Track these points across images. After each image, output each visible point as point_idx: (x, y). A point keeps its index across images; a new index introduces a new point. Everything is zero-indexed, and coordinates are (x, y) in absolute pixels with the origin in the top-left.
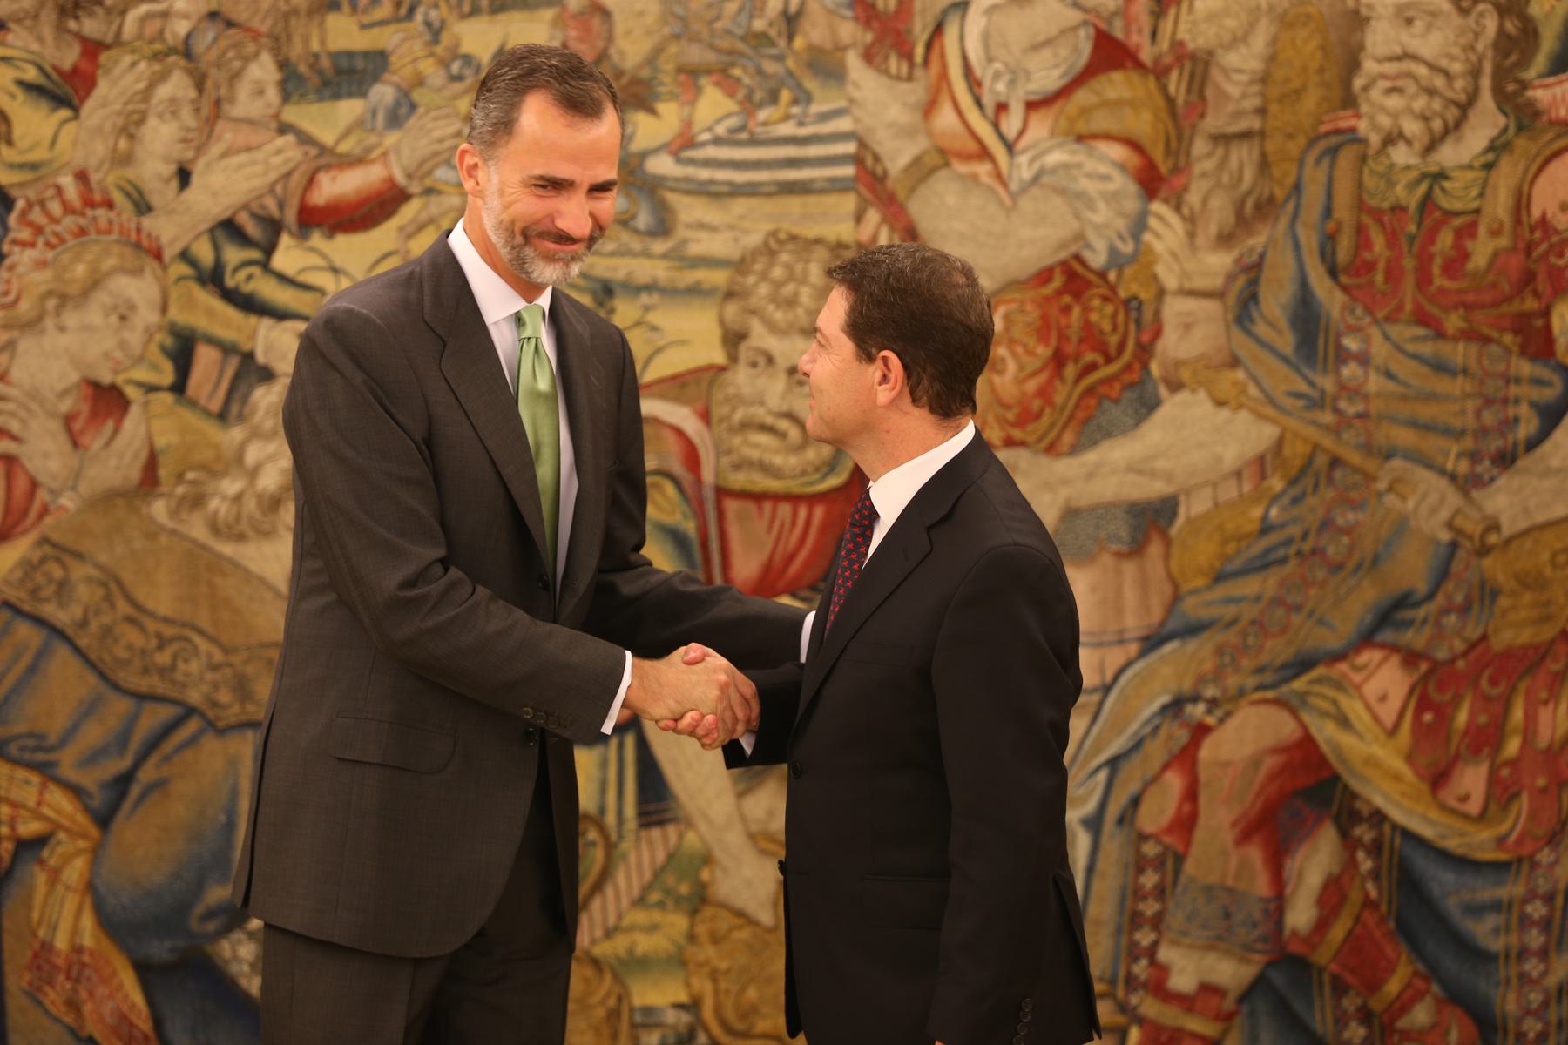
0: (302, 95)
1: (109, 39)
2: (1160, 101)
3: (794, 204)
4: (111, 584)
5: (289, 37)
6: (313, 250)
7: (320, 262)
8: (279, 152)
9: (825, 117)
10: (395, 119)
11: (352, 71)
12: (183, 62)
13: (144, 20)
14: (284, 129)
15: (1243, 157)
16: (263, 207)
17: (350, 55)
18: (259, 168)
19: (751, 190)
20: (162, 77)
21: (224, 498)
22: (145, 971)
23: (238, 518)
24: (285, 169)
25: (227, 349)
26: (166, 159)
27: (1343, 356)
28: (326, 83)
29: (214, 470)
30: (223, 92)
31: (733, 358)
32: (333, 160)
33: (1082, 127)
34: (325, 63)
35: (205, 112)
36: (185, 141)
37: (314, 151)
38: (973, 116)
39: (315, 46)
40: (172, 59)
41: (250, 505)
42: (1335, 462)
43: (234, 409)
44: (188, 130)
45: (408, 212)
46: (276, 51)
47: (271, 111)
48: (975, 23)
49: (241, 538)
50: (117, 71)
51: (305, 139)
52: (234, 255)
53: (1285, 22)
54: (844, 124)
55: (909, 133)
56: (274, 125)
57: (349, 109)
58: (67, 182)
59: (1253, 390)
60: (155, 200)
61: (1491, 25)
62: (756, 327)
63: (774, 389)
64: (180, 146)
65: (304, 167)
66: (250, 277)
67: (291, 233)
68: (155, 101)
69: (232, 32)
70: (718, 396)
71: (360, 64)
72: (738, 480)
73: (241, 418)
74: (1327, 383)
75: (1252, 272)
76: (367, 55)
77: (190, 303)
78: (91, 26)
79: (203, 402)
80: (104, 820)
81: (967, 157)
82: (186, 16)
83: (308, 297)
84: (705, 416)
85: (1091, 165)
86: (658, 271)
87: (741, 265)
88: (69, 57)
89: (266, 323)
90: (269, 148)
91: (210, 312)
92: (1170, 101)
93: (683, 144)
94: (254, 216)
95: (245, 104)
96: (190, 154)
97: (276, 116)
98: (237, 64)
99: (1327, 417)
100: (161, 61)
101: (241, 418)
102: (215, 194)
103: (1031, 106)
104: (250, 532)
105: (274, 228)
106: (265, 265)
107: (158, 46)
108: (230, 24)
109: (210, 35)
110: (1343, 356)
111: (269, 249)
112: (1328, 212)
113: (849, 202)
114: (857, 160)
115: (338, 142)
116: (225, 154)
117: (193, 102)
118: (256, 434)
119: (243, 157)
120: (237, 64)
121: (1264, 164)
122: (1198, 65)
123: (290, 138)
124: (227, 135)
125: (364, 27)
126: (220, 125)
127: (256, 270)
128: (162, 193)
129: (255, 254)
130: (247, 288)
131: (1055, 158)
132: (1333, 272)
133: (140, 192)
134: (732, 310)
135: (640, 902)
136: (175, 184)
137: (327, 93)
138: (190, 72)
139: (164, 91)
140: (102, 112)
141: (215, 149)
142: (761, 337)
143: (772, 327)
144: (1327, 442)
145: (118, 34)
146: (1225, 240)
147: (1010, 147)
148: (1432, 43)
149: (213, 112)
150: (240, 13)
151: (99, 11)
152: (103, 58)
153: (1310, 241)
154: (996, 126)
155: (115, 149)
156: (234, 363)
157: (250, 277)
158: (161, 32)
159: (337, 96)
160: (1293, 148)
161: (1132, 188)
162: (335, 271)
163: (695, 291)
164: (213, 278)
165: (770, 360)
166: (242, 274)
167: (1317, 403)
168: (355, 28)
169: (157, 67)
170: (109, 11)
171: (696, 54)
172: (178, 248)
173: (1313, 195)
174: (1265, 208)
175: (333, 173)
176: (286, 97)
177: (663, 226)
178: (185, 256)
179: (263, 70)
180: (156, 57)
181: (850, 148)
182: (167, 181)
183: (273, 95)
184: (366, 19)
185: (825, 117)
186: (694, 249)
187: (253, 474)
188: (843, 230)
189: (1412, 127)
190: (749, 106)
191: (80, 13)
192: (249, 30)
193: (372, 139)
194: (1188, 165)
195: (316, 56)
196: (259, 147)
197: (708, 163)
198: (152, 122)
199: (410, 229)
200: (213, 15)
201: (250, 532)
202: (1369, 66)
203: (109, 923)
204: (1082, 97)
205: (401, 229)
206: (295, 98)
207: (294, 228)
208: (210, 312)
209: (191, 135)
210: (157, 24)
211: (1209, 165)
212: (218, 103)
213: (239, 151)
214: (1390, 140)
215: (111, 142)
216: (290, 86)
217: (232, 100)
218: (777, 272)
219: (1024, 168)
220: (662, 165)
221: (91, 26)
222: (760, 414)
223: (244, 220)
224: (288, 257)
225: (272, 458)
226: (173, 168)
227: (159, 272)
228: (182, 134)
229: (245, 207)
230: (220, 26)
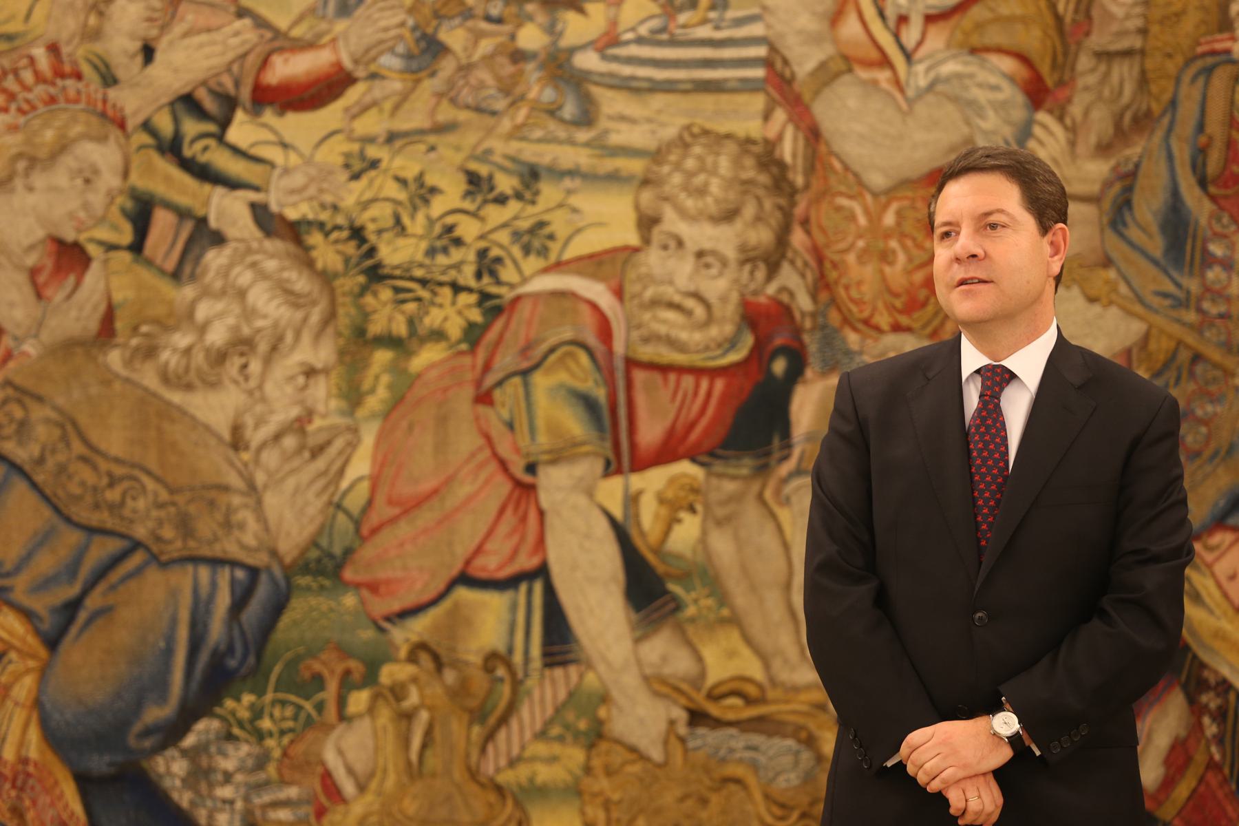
2: (1049, 20)
3: (708, 102)
4: (68, 425)
7: (271, 137)
9: (739, 22)
15: (1124, 73)
16: (220, 84)
19: (668, 87)
21: (175, 350)
22: (84, 782)
23: (187, 369)
24: (241, 50)
25: (183, 214)
26: (132, 36)
27: (1209, 260)
29: (167, 325)
31: (647, 241)
32: (286, 44)
33: (975, 40)
36: (150, 20)
37: (269, 35)
41: (199, 358)
42: (1197, 358)
43: (187, 269)
44: (154, 10)
45: (353, 95)
49: (189, 387)
51: (261, 23)
52: (191, 127)
54: (757, 30)
55: (814, 39)
58: (40, 53)
59: (1123, 289)
60: (120, 73)
62: (669, 214)
63: (683, 271)
65: (258, 50)
66: (206, 149)
67: (245, 109)
70: (631, 274)
72: (646, 352)
73: (193, 277)
74: (1193, 285)
75: (1127, 179)
77: (149, 170)
79: (158, 261)
80: (52, 642)
81: (868, 64)
83: (258, 168)
84: (619, 293)
85: (983, 76)
86: (581, 158)
87: (657, 156)
89: (220, 191)
90: (228, 30)
91: (168, 179)
92: (1059, 19)
93: (608, 42)
94: (212, 92)
96: (154, 32)
99: (1191, 316)
101: (193, 277)
102: (176, 71)
103: (930, 19)
104: (197, 382)
105: (230, 104)
106: (220, 138)
110: (1209, 260)
111: (225, 123)
112: (1201, 128)
113: (758, 102)
114: (767, 63)
118: (206, 293)
119: (204, 38)
121: (1143, 81)
123: (247, 22)
127: (212, 142)
128: (127, 67)
129: (211, 127)
130: (203, 158)
131: (949, 68)
132: (1203, 183)
133: (107, 66)
134: (647, 196)
135: (542, 735)
136: (139, 59)
141: (178, 29)
142: (672, 222)
143: (683, 213)
144: (1190, 339)
146: (1103, 149)
147: (908, 56)
153: (1182, 153)
154: (897, 36)
156: (188, 227)
157: (206, 149)
160: (1171, 67)
161: (1020, 98)
162: (285, 146)
163: (614, 178)
164: (172, 148)
165: (680, 243)
166: (199, 146)
167: (1182, 303)
172: (140, 119)
173: (1188, 111)
174: (1142, 122)
175: (287, 55)
177: (586, 118)
178: (147, 126)
181: (761, 51)
182: (133, 56)
185: (739, 22)
186: (615, 139)
187: (203, 329)
188: (752, 127)
193: (323, 26)
194: (1073, 79)
196: (218, 28)
197: (631, 60)
199: (355, 110)
201: (197, 382)
203: (54, 738)
205: (347, 110)
207: (248, 104)
208: (168, 179)
211: (1091, 79)
218: (690, 163)
219: (920, 77)
220: (588, 61)
222: (669, 292)
223: (203, 95)
224: (241, 131)
225: (220, 315)
226: (138, 45)
227: (122, 140)
229: (204, 83)
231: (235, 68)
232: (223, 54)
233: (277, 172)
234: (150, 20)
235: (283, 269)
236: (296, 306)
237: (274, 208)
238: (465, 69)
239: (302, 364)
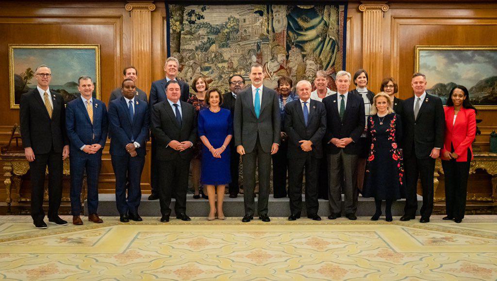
10: (212, 73)
20: (189, 69)
38: (268, 73)
48: (269, 64)
53: (299, 65)
57: (207, 72)
61: (319, 65)
78: (183, 64)
88: (181, 66)
95: (197, 71)
103: (274, 72)
122: (290, 69)
128: (189, 80)
139: (189, 70)
148: (313, 67)
149: (194, 72)
171: (241, 67)
179: (199, 68)
189: (311, 75)
190: (246, 72)
202: (307, 69)
204: (279, 72)
214: (309, 77)
221: (183, 64)
238: (225, 79)
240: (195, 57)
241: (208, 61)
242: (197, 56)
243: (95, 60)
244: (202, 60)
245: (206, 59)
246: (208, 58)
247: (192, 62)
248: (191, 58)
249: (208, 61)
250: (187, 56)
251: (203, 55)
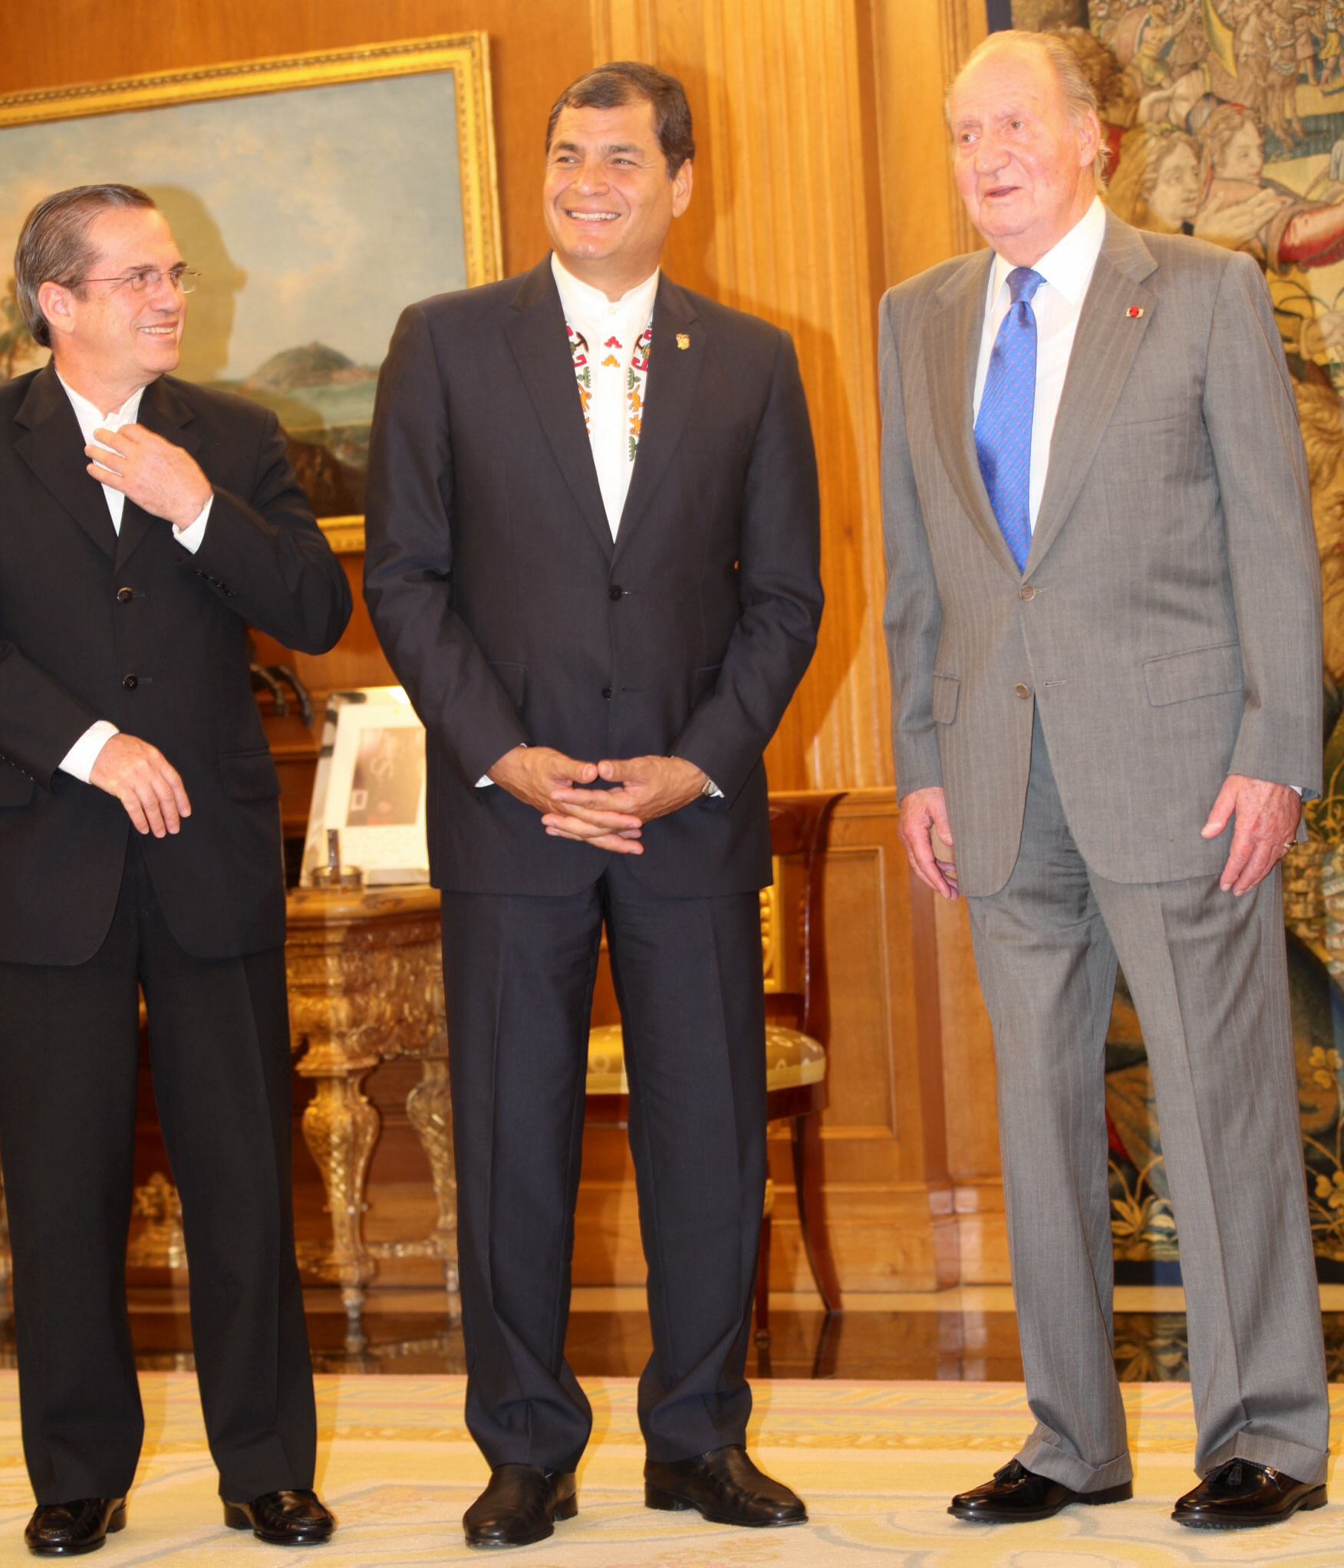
0: (1278, 156)
1: (1128, 123)
5: (1267, 108)
6: (1292, 282)
7: (1300, 293)
8: (1261, 204)
11: (1318, 132)
12: (1185, 137)
13: (1152, 106)
14: (1265, 183)
17: (1317, 118)
18: (1246, 218)
20: (1168, 150)
28: (1298, 144)
30: (1216, 158)
32: (1305, 207)
34: (1296, 126)
35: (1203, 175)
36: (1187, 200)
37: (1289, 201)
39: (1288, 114)
40: (1176, 134)
44: (1191, 191)
46: (1257, 121)
47: (1255, 170)
50: (1134, 148)
51: (1282, 191)
56: (1257, 182)
57: (1317, 163)
64: (1185, 205)
67: (1273, 270)
68: (1163, 170)
69: (1222, 108)
71: (1324, 125)
76: (1329, 116)
82: (1186, 99)
83: (1290, 321)
90: (1254, 200)
96: (1192, 211)
97: (1259, 174)
98: (1226, 134)
100: (1166, 138)
107: (1165, 125)
108: (1221, 102)
109: (1205, 113)
115: (1308, 192)
116: (1218, 210)
117: (1193, 168)
119: (1233, 210)
120: (1226, 134)
123: (1270, 191)
124: (1220, 193)
125: (1326, 94)
126: (1216, 185)
137: (1299, 152)
138: (1191, 145)
139: (1170, 162)
140: (1124, 183)
141: (1212, 205)
145: (1135, 118)
150: (1227, 93)
151: (1120, 101)
152: (1125, 139)
155: (1134, 212)
158: (1167, 114)
159: (1307, 154)
168: (1320, 95)
169: (1164, 142)
170: (1127, 101)
175: (1307, 217)
176: (1266, 158)
179: (1248, 137)
180: (1164, 134)
183: (1255, 157)
184: (1328, 88)
191: (1107, 104)
192: (1235, 105)
195: (1289, 122)
196: (1245, 201)
198: (1162, 187)
200: (1208, 96)
206: (1273, 158)
207: (1276, 265)
209: (1192, 196)
210: (1163, 107)
212: (1212, 167)
213: (1229, 206)
215: (1131, 207)
216: (1269, 149)
217: (1223, 164)
228: (1186, 195)
230: (1213, 103)
231: (1262, 234)
232: (1251, 222)
233: (1305, 323)
234: (1187, 200)
235: (1317, 410)
236: (1330, 442)
237: (1305, 356)
239: (1337, 495)
240: (1211, 46)
241: (1317, 62)
242: (1223, 36)
243: (460, 154)
244: (1266, 67)
245: (1304, 51)
246: (1315, 42)
247: (1187, 87)
248: (1177, 56)
249: (1317, 62)
250: (1149, 51)
251: (1279, 24)
